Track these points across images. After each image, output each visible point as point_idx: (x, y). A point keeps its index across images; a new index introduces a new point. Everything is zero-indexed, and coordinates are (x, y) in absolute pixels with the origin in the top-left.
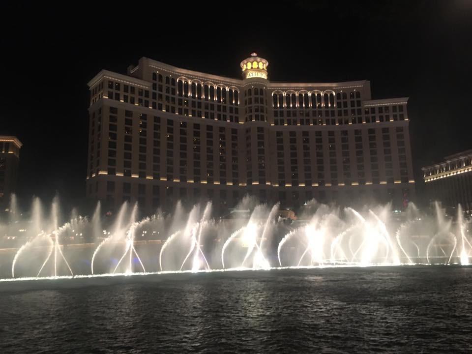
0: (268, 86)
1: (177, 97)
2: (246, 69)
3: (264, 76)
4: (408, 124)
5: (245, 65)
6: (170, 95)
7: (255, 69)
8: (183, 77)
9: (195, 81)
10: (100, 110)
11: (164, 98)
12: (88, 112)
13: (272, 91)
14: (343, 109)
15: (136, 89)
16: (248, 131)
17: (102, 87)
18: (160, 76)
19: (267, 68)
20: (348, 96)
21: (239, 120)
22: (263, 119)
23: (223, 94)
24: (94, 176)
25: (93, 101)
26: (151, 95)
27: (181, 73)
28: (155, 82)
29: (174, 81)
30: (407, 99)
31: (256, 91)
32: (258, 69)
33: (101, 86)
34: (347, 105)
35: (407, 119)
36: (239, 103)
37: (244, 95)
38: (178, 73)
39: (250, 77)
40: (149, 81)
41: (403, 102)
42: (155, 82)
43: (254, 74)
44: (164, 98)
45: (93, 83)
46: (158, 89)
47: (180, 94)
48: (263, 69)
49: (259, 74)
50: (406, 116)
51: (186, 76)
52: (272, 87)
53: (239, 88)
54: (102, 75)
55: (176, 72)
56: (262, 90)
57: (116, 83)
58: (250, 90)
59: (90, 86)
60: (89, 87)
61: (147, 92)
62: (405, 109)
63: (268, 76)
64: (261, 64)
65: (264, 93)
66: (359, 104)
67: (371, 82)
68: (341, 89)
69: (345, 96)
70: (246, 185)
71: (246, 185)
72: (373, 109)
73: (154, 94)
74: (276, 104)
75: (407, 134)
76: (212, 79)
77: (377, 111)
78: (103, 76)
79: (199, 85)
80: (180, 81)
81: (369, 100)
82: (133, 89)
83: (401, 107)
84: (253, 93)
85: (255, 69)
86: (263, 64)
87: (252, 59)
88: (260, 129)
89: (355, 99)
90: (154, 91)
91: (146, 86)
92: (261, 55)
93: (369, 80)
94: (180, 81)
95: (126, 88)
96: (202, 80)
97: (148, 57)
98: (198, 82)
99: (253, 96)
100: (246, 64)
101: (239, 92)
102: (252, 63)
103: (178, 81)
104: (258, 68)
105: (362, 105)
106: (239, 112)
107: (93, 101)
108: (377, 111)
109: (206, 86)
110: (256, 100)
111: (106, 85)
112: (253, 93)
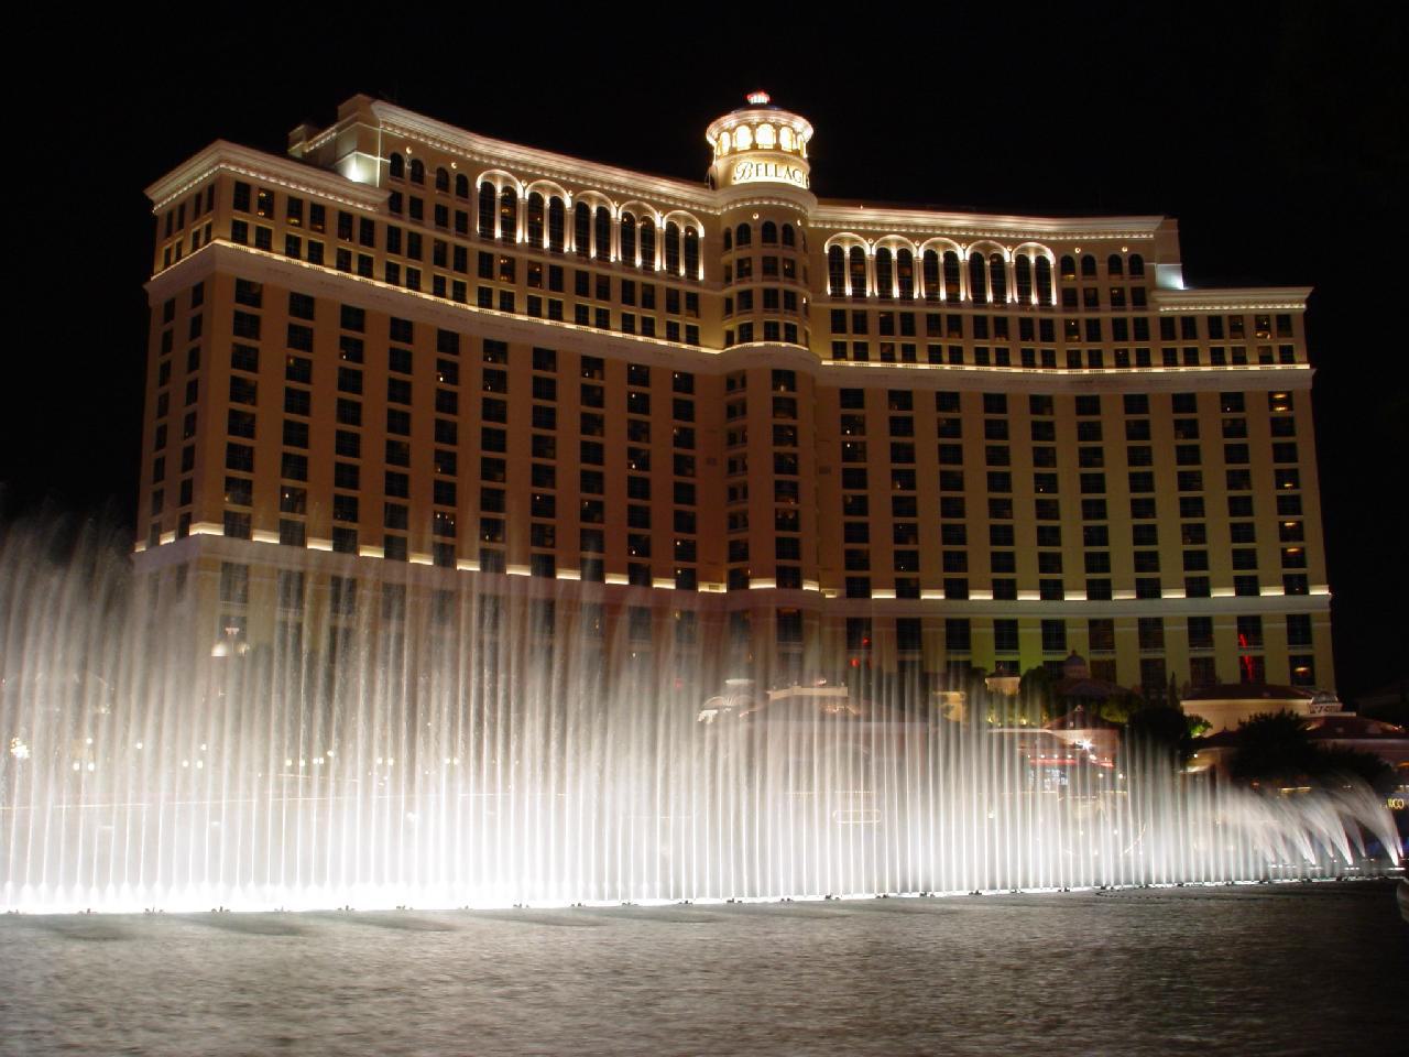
0: (810, 214)
1: (474, 246)
2: (733, 151)
3: (798, 177)
4: (1309, 385)
5: (725, 136)
7: (762, 147)
8: (498, 171)
10: (198, 294)
11: (428, 251)
12: (146, 295)
13: (826, 234)
14: (1082, 315)
15: (327, 212)
16: (736, 381)
17: (210, 207)
19: (811, 145)
20: (1102, 266)
21: (701, 340)
22: (791, 338)
24: (168, 539)
25: (168, 252)
26: (381, 237)
27: (491, 157)
29: (464, 184)
30: (1305, 292)
31: (767, 235)
33: (205, 199)
35: (1307, 367)
36: (701, 276)
37: (721, 241)
38: (481, 155)
39: (743, 181)
41: (1291, 302)
43: (762, 167)
45: (170, 191)
48: (797, 153)
49: (783, 170)
50: (1300, 353)
51: (512, 165)
52: (824, 222)
53: (704, 218)
54: (214, 158)
55: (473, 152)
56: (789, 232)
57: (261, 190)
58: (744, 231)
59: (154, 198)
60: (151, 204)
61: (368, 225)
62: (1298, 328)
63: (813, 177)
64: (785, 134)
65: (798, 238)
67: (1180, 227)
68: (1077, 244)
69: (1089, 264)
70: (723, 590)
71: (723, 590)
74: (838, 283)
76: (602, 182)
77: (1202, 329)
78: (220, 161)
79: (557, 203)
80: (488, 188)
83: (1284, 321)
84: (756, 235)
85: (762, 147)
86: (798, 132)
87: (755, 116)
88: (783, 377)
89: (1127, 282)
91: (365, 202)
92: (781, 101)
93: (1173, 217)
94: (488, 188)
95: (295, 206)
96: (567, 186)
97: (377, 95)
99: (756, 251)
100: (732, 131)
101: (701, 233)
102: (753, 127)
103: (479, 184)
104: (778, 147)
105: (1149, 305)
106: (702, 309)
107: (168, 252)
108: (1202, 329)
109: (581, 209)
110: (770, 267)
111: (227, 196)
112: (756, 235)
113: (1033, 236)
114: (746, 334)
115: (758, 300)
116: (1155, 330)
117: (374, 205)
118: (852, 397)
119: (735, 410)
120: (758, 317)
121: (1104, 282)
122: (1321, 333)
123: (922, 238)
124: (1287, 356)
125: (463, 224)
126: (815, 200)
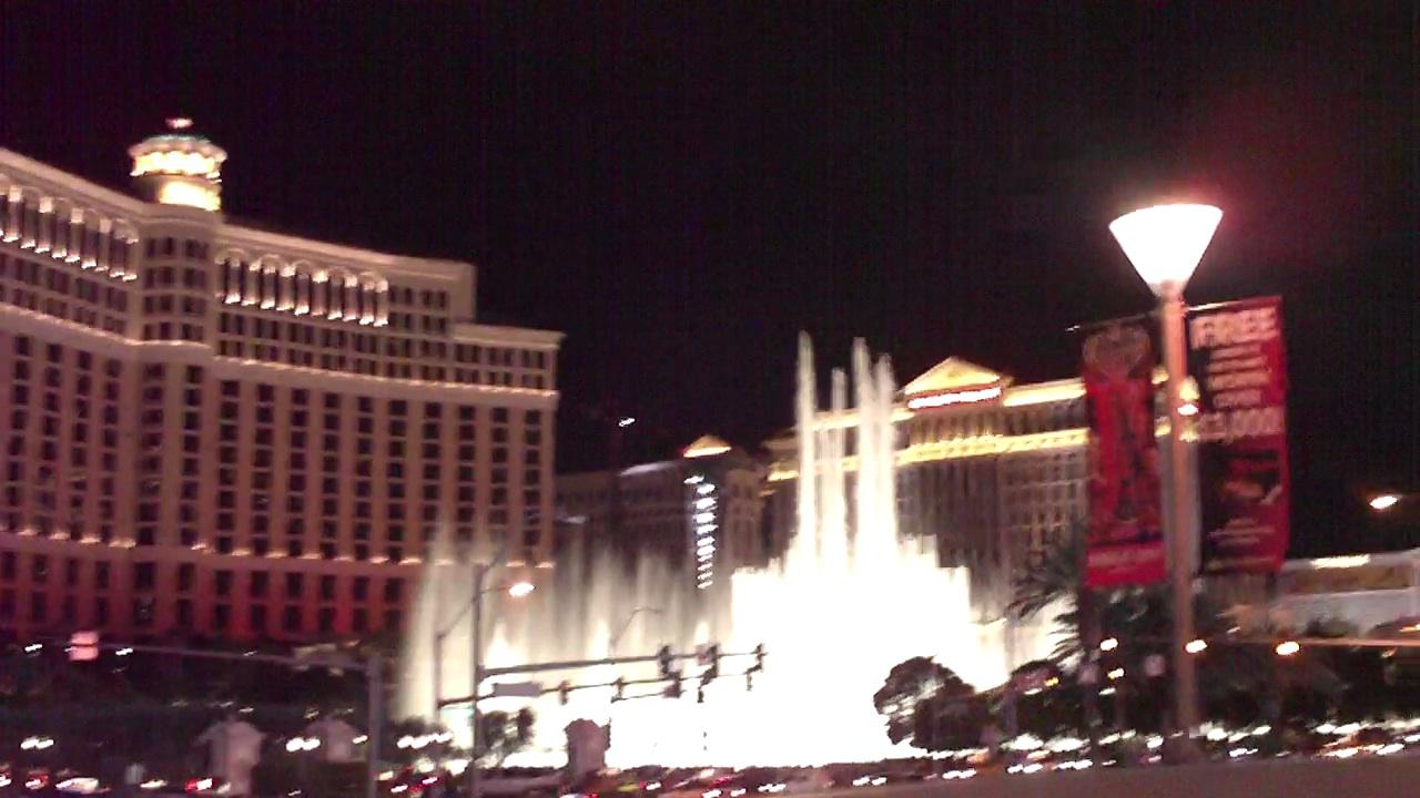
3: (210, 201)
14: (402, 334)
32: (200, 178)
34: (415, 336)
41: (546, 342)
66: (442, 325)
72: (476, 349)
75: (546, 428)
81: (460, 321)
83: (541, 355)
85: (184, 171)
86: (206, 160)
113: (374, 269)
114: (165, 332)
115: (177, 304)
116: (451, 352)
118: (231, 387)
119: (155, 394)
120: (177, 318)
121: (418, 311)
122: (569, 370)
123: (290, 260)
124: (540, 385)
126: (221, 217)
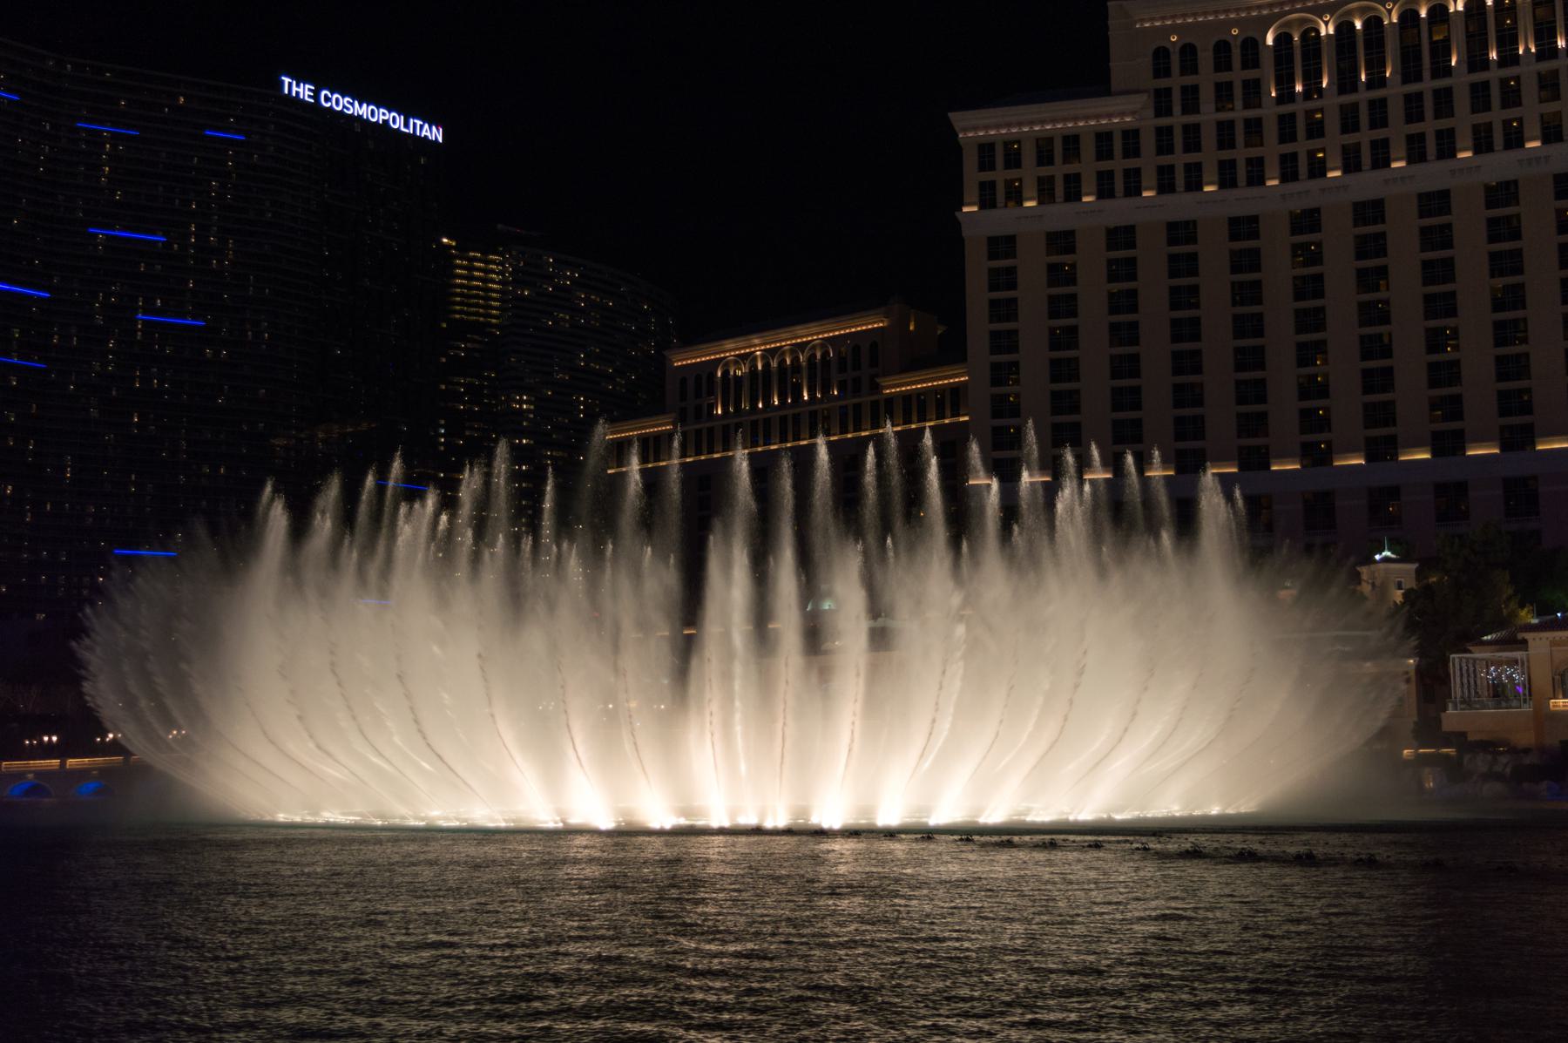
1: (1269, 112)
6: (1239, 114)
9: (1288, 24)
18: (1188, 51)
23: (1419, 58)
26: (1148, 143)
28: (1163, 83)
29: (1252, 46)
40: (1137, 92)
42: (1163, 83)
44: (1209, 138)
46: (1177, 109)
47: (1287, 96)
61: (1131, 138)
73: (1164, 134)
82: (1072, 143)
90: (1164, 121)
91: (1122, 114)
98: (1362, 11)
103: (1270, 40)
117: (1133, 113)
125: (1253, 91)
